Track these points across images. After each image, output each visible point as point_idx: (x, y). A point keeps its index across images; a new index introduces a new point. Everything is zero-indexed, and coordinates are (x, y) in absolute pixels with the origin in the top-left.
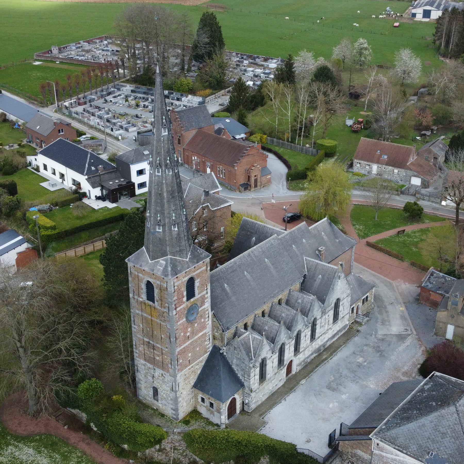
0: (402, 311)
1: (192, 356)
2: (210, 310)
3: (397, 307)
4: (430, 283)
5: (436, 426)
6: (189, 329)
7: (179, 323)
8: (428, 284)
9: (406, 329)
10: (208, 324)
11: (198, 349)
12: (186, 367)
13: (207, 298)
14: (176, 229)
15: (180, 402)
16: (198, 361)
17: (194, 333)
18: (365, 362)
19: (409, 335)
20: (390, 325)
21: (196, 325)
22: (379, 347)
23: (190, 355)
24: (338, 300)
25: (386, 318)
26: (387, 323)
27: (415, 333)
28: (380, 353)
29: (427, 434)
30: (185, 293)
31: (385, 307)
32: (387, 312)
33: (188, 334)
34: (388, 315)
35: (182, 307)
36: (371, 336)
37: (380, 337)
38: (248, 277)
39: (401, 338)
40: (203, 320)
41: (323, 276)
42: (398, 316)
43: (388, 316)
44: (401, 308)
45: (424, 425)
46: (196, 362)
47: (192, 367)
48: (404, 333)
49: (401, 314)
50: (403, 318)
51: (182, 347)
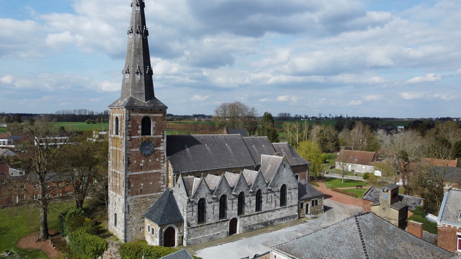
1: (144, 186)
2: (165, 154)
4: (370, 196)
5: (333, 236)
6: (143, 161)
7: (132, 150)
8: (369, 197)
10: (163, 166)
11: (151, 183)
12: (137, 194)
13: (163, 142)
14: (139, 77)
15: (129, 224)
16: (151, 194)
17: (147, 166)
21: (150, 160)
23: (142, 184)
24: (284, 187)
29: (323, 244)
30: (140, 127)
33: (142, 165)
35: (136, 137)
38: (208, 148)
40: (157, 160)
41: (272, 165)
45: (321, 236)
46: (148, 195)
47: (144, 197)
51: (134, 173)
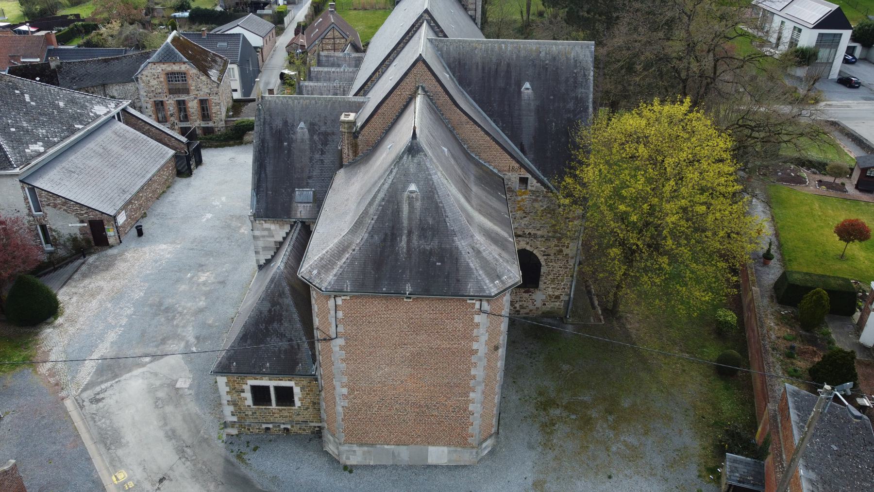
0: (115, 464)
3: (139, 474)
9: (98, 401)
18: (192, 277)
19: (85, 390)
20: (152, 390)
22: (170, 320)
25: (169, 409)
26: (161, 394)
27: (69, 404)
28: (163, 308)
31: (181, 452)
32: (172, 435)
34: (166, 424)
36: (197, 338)
37: (173, 346)
39: (113, 368)
42: (129, 436)
43: (164, 419)
44: (122, 475)
48: (109, 384)
49: (120, 452)
50: (110, 439)
